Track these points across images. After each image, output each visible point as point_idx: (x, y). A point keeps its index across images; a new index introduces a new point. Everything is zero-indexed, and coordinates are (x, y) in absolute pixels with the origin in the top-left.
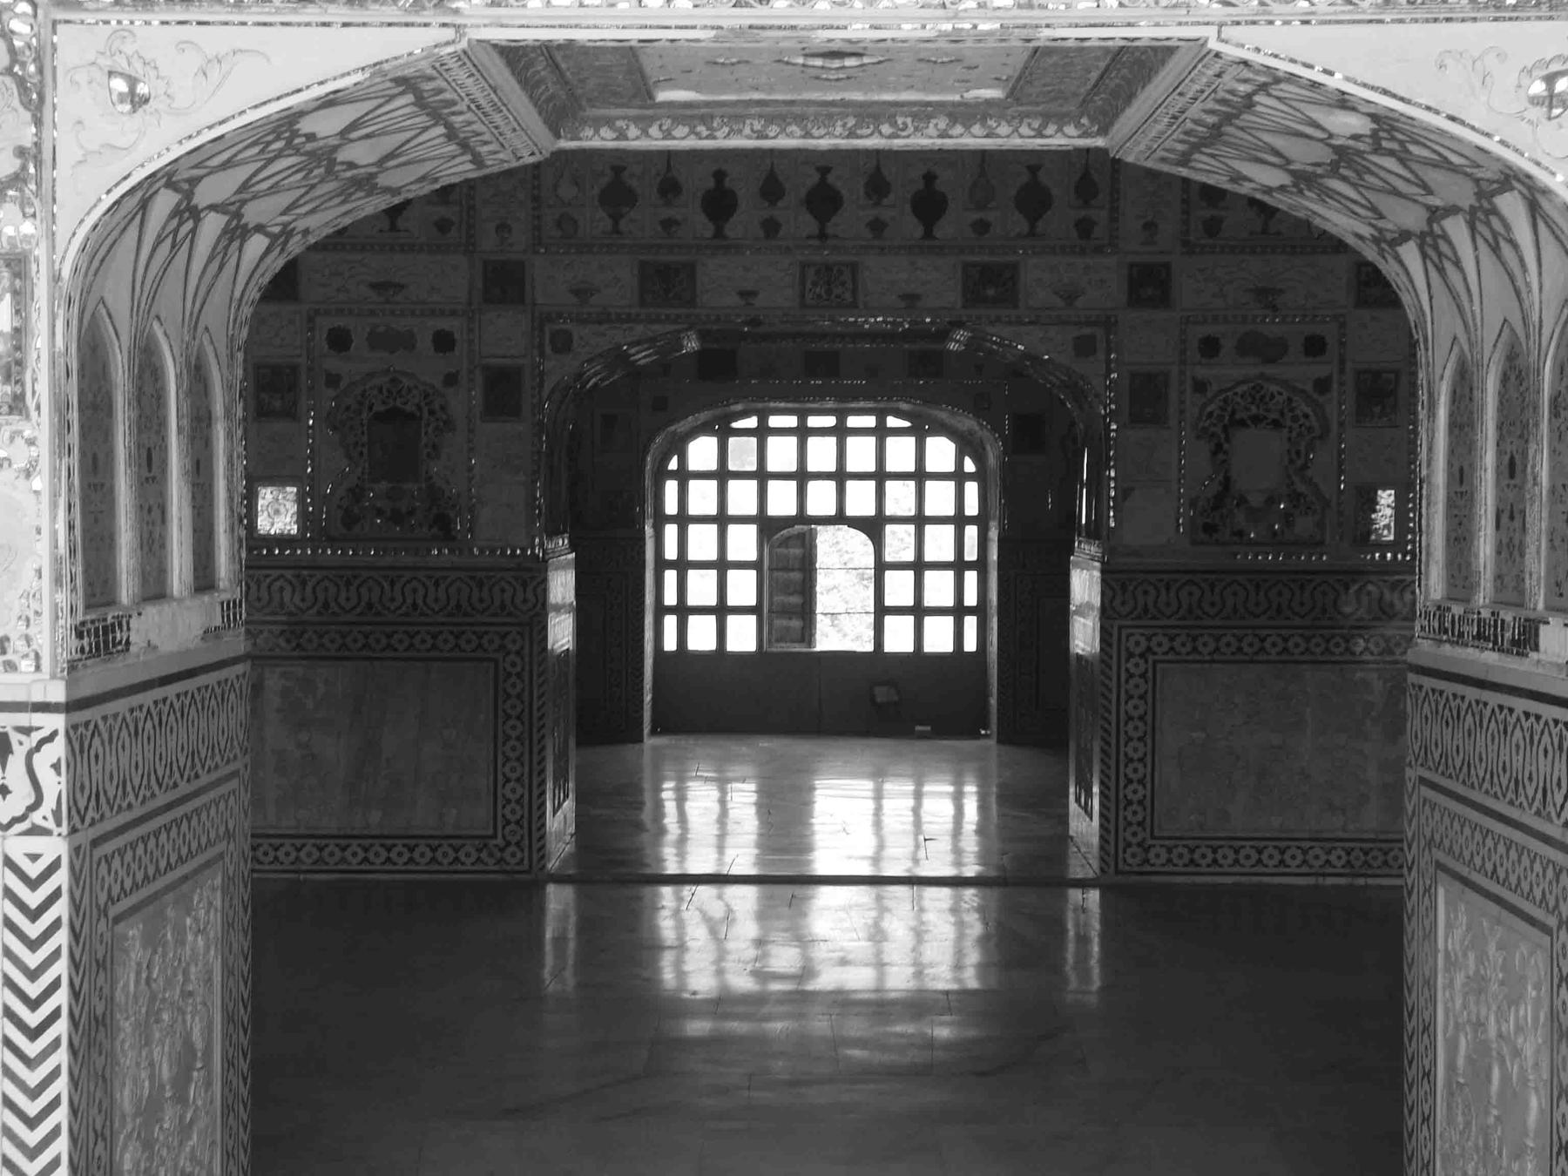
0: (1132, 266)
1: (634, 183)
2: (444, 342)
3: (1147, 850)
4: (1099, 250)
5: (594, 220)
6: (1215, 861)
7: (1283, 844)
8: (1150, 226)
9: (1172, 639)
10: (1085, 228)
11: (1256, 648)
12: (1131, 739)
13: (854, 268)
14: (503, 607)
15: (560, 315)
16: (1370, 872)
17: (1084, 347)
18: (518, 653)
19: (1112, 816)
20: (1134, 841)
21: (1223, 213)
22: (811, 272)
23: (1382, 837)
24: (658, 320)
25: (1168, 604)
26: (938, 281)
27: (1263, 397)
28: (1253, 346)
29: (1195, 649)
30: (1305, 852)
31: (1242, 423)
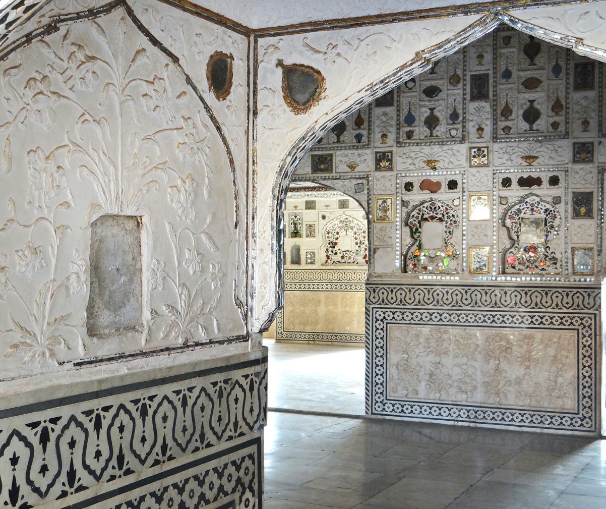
0: (377, 153)
3: (384, 405)
4: (364, 147)
6: (412, 411)
7: (441, 406)
8: (384, 136)
9: (394, 314)
10: (359, 138)
11: (428, 319)
12: (377, 356)
16: (478, 421)
19: (370, 389)
20: (379, 400)
21: (415, 129)
23: (482, 405)
25: (392, 299)
27: (435, 208)
29: (403, 318)
30: (449, 410)
31: (426, 219)
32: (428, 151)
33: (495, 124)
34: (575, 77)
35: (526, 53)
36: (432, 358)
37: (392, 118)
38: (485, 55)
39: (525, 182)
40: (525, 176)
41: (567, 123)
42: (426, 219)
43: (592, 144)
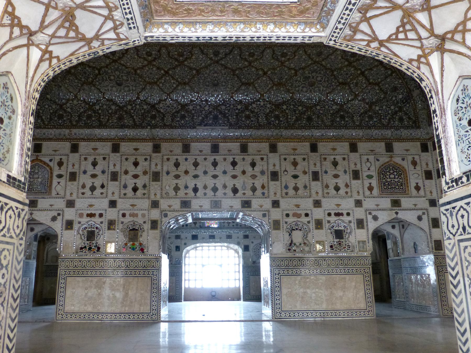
1: (180, 186)
2: (143, 215)
4: (266, 198)
5: (172, 193)
8: (275, 194)
10: (263, 194)
13: (221, 201)
14: (153, 266)
15: (165, 210)
17: (264, 215)
18: (156, 275)
22: (213, 203)
24: (184, 211)
26: (237, 203)
28: (295, 215)
31: (294, 230)
32: (295, 201)
33: (323, 191)
34: (353, 175)
35: (333, 165)
36: (302, 290)
37: (278, 186)
38: (317, 164)
39: (337, 214)
40: (337, 212)
41: (351, 192)
42: (294, 230)
43: (361, 200)
